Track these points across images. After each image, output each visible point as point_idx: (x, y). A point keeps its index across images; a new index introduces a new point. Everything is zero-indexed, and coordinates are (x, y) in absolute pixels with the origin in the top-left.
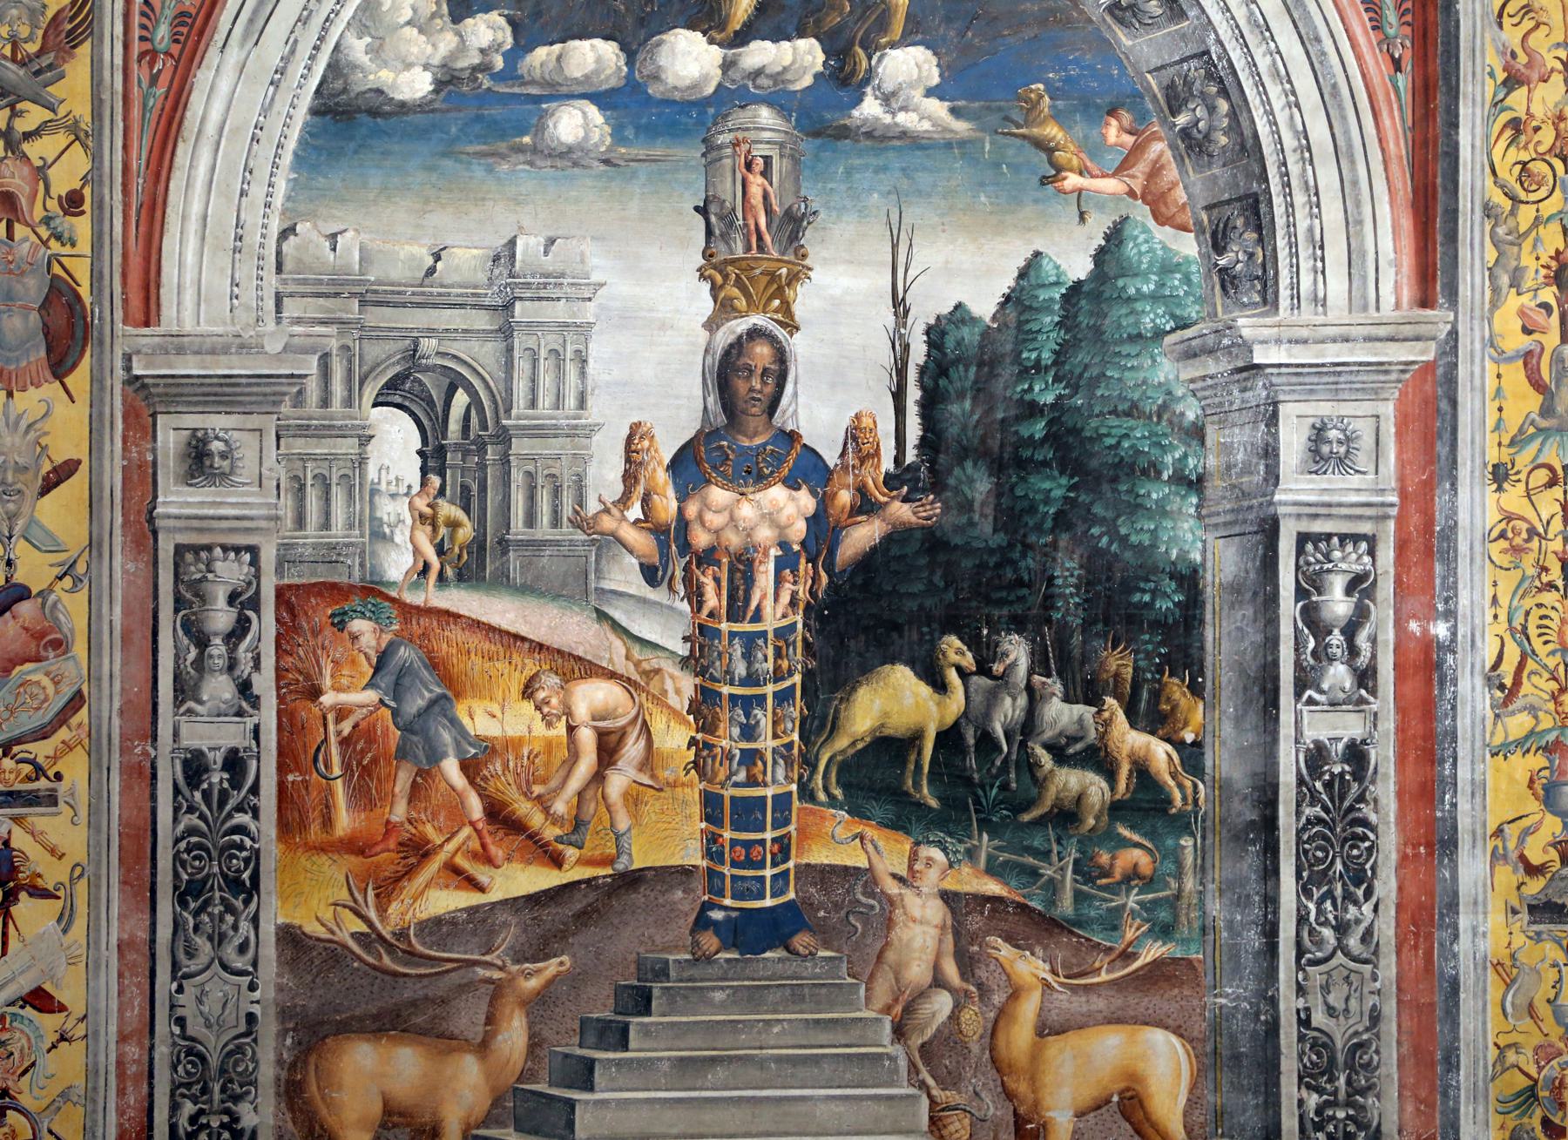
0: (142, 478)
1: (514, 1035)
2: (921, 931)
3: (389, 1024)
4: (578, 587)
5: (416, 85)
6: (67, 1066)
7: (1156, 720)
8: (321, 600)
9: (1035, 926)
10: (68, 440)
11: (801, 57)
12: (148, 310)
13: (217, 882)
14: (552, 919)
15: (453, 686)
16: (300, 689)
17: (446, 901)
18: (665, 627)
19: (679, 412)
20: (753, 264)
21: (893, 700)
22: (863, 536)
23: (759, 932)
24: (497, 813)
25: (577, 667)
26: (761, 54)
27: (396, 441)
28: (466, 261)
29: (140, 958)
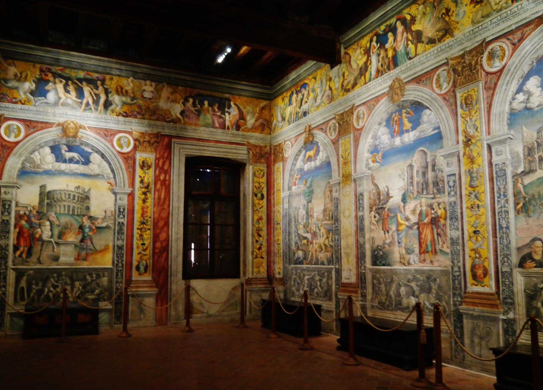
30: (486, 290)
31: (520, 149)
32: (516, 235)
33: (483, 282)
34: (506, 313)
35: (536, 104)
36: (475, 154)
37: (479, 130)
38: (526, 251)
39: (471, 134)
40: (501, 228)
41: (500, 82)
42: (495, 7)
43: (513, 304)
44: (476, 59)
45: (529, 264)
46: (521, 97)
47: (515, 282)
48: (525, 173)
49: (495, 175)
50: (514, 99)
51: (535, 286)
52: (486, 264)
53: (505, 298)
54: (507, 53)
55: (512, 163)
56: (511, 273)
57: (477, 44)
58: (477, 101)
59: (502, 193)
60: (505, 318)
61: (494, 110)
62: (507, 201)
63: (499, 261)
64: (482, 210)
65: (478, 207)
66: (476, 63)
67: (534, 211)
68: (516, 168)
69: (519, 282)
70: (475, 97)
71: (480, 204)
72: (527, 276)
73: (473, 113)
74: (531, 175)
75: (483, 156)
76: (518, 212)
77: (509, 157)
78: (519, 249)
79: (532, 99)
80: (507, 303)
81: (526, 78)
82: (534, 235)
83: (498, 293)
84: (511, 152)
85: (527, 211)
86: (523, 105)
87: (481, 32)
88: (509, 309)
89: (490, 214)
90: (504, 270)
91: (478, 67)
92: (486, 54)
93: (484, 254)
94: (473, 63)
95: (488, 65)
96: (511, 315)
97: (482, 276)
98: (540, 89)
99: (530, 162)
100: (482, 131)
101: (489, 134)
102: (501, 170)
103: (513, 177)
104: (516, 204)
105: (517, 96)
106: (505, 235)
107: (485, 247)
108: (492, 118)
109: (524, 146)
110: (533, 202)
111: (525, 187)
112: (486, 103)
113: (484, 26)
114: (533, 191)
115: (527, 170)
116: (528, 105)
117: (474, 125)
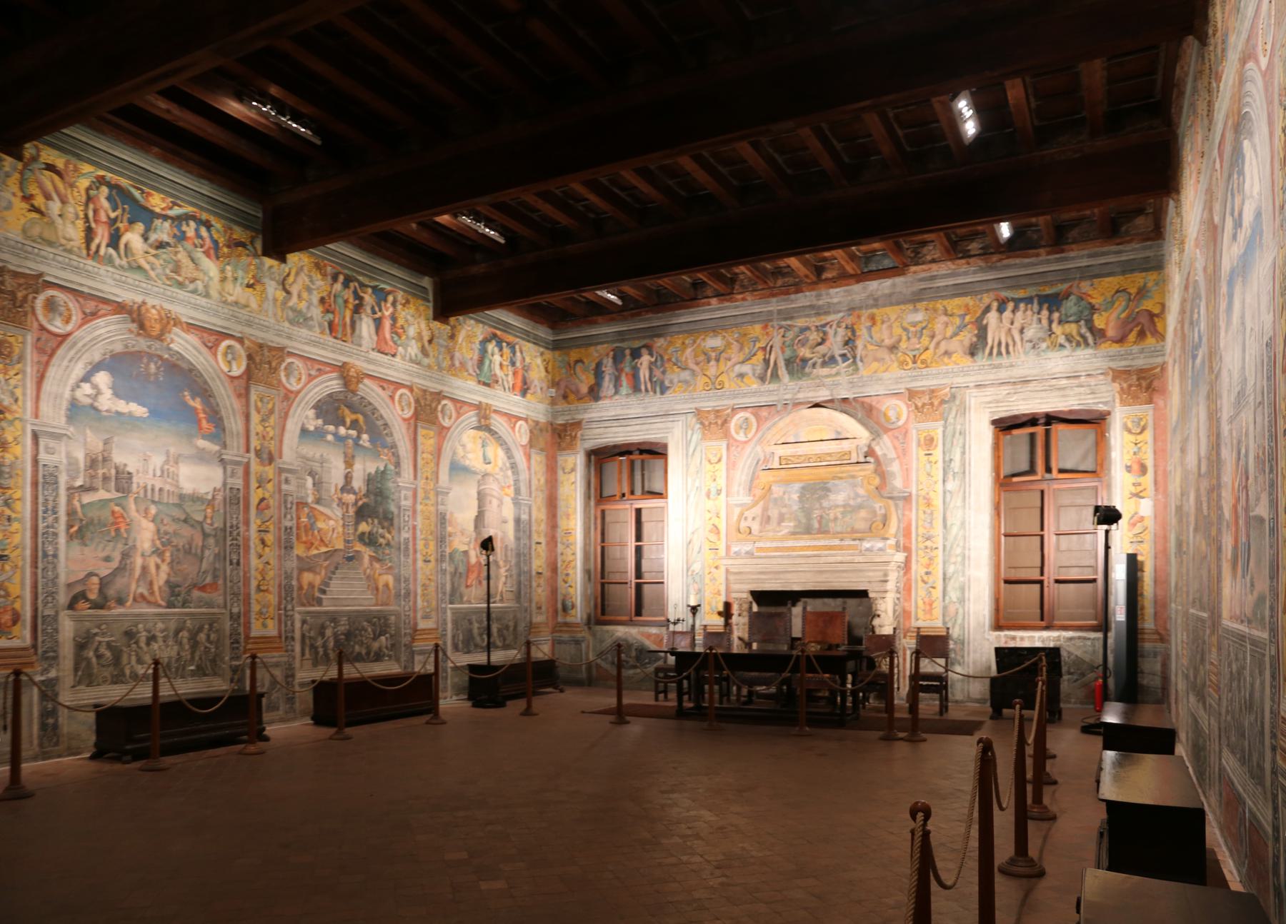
0: (280, 482)
1: (323, 572)
2: (366, 560)
3: (310, 570)
4: (328, 506)
5: (312, 428)
6: (271, 574)
7: (389, 532)
8: (301, 504)
9: (378, 560)
10: (271, 476)
11: (353, 433)
12: (281, 457)
13: (289, 547)
14: (329, 555)
15: (316, 520)
16: (299, 518)
17: (316, 552)
18: (339, 512)
19: (341, 483)
20: (349, 463)
21: (364, 527)
22: (360, 503)
23: (350, 559)
24: (322, 540)
25: (330, 518)
26: (351, 432)
27: (310, 481)
28: (318, 455)
29: (280, 557)
30: (16, 643)
31: (80, 455)
32: (67, 567)
33: (10, 633)
34: (46, 671)
35: (105, 408)
36: (10, 439)
37: (20, 403)
38: (79, 589)
39: (6, 403)
40: (45, 555)
41: (60, 352)
42: (63, 241)
43: (55, 658)
44: (25, 292)
45: (82, 605)
46: (87, 388)
47: (60, 628)
48: (85, 489)
49: (41, 480)
50: (78, 387)
51: (88, 631)
52: (17, 606)
53: (46, 652)
54: (74, 318)
55: (68, 471)
56: (55, 618)
57: (28, 272)
58: (21, 359)
59: (50, 507)
60: (43, 678)
61: (48, 386)
62: (56, 520)
63: (40, 601)
64: (16, 526)
65: (9, 519)
66: (25, 299)
67: (92, 539)
68: (74, 478)
69: (67, 628)
70: (17, 351)
71: (13, 515)
72: (78, 620)
73: (12, 373)
74: (91, 493)
75: (24, 446)
76: (71, 537)
77: (65, 461)
78: (69, 586)
79: (101, 398)
80: (47, 658)
81: (97, 367)
82: (90, 569)
83: (35, 646)
84: (68, 456)
85: (82, 538)
86: (89, 401)
87: (39, 259)
88: (51, 666)
89: (28, 534)
90: (47, 613)
91: (27, 307)
92: (41, 298)
93: (14, 590)
94: (20, 295)
95: (45, 316)
96: (53, 674)
97: (10, 624)
98: (110, 392)
99: (92, 477)
100: (24, 409)
101: (37, 416)
102: (51, 475)
103: (68, 489)
104: (70, 526)
105: (83, 384)
106: (50, 566)
107: (17, 579)
108: (43, 396)
109: (87, 455)
110: (91, 528)
111: (82, 506)
112: (35, 369)
113: (43, 253)
114: (93, 514)
115: (88, 485)
116: (96, 404)
117: (12, 394)
